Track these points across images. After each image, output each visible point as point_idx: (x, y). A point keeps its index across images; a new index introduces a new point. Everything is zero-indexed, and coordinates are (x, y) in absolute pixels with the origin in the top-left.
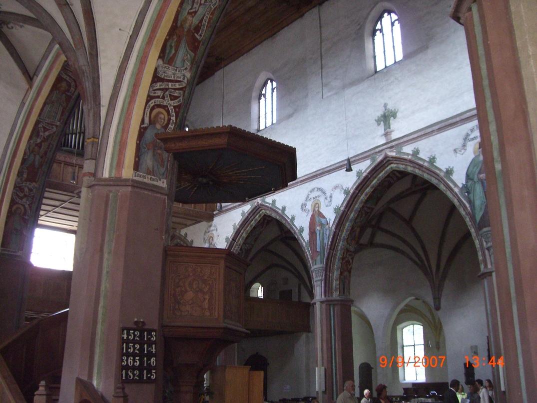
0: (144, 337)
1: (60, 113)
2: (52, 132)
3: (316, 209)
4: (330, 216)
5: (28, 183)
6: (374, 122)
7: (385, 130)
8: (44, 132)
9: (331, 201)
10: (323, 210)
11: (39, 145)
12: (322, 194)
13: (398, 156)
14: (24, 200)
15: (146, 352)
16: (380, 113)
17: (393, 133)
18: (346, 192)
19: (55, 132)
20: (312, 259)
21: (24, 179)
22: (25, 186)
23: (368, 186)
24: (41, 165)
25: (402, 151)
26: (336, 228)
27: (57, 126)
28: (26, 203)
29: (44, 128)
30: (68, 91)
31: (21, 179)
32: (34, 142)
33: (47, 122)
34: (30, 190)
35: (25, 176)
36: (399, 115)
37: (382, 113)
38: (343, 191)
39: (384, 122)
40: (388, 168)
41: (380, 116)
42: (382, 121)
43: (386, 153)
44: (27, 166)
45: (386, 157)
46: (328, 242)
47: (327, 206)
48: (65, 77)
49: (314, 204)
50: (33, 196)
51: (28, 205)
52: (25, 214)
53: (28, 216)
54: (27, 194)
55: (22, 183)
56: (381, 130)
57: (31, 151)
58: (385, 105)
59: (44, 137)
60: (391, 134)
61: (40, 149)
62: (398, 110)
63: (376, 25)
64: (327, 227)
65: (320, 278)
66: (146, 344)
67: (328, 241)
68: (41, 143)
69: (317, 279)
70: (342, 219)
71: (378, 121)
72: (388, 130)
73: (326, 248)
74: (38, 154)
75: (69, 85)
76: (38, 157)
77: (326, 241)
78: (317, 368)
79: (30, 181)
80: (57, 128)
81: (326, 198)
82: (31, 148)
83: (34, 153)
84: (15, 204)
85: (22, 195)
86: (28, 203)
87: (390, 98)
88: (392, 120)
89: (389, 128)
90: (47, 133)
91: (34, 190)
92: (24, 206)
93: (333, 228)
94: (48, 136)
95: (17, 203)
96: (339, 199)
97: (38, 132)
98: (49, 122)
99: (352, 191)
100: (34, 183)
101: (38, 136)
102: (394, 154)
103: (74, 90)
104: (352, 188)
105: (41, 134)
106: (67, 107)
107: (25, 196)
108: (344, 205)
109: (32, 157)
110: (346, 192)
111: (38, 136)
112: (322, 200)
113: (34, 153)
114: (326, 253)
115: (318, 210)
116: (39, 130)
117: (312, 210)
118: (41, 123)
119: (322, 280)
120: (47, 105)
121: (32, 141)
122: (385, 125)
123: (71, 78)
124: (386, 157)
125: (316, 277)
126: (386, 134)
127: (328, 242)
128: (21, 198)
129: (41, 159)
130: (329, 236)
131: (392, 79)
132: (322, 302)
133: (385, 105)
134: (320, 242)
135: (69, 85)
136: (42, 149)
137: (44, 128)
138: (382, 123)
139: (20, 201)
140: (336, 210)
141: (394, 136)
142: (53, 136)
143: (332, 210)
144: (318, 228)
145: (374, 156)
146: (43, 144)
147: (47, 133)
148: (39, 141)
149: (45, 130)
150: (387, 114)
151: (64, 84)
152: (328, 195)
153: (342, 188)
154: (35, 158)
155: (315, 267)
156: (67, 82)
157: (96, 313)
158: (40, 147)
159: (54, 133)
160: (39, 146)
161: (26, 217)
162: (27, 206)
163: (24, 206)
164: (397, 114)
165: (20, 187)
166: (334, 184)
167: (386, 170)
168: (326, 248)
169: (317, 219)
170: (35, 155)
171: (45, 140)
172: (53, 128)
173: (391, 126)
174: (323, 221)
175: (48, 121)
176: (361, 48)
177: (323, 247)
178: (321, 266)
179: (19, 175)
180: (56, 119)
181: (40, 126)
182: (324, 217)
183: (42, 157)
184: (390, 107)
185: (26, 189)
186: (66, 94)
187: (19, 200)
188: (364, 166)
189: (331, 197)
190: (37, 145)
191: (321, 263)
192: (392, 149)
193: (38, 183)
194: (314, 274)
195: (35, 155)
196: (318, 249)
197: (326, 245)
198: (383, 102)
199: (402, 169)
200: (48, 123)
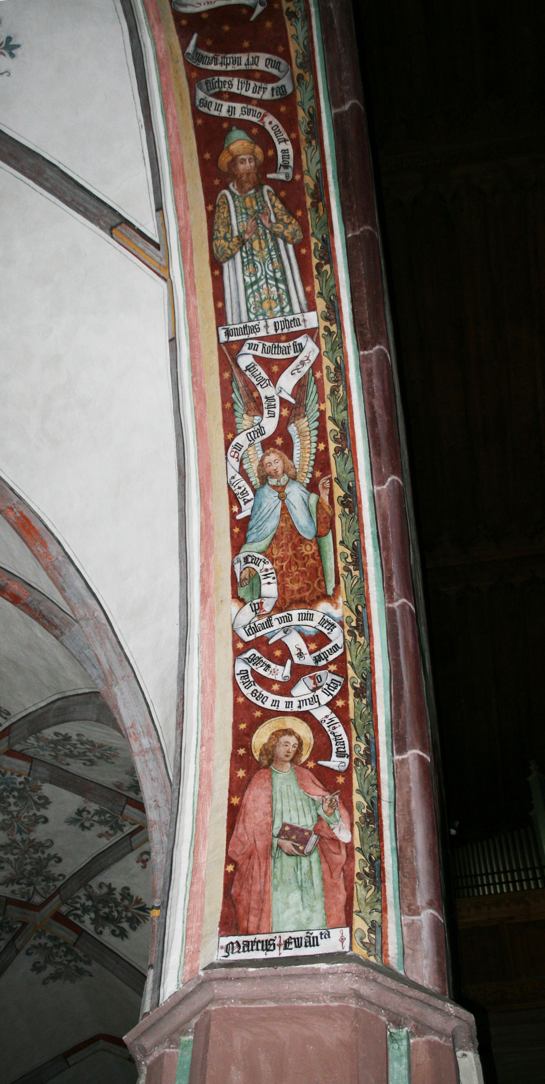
2: (305, 369)
5: (295, 613)
8: (274, 378)
11: (279, 441)
14: (302, 690)
19: (319, 357)
21: (268, 606)
22: (286, 631)
24: (325, 523)
27: (311, 333)
28: (315, 700)
29: (265, 363)
30: (270, 163)
31: (257, 609)
32: (252, 441)
33: (262, 333)
34: (320, 640)
35: (270, 590)
44: (263, 545)
48: (224, 109)
50: (341, 661)
51: (328, 704)
52: (323, 748)
53: (340, 754)
54: (308, 660)
57: (255, 480)
59: (282, 401)
61: (291, 457)
68: (282, 430)
74: (294, 478)
75: (262, 139)
76: (296, 494)
79: (299, 603)
80: (318, 343)
84: (254, 725)
85: (281, 673)
86: (325, 699)
90: (288, 381)
91: (337, 636)
92: (306, 716)
94: (301, 387)
95: (268, 715)
97: (250, 389)
98: (272, 331)
100: (324, 606)
101: (256, 406)
103: (288, 146)
105: (266, 392)
106: (305, 230)
107: (299, 672)
109: (270, 499)
111: (256, 406)
113: (273, 482)
116: (248, 383)
118: (245, 349)
120: (227, 267)
121: (241, 439)
123: (247, 100)
128: (286, 689)
129: (314, 497)
135: (262, 139)
137: (265, 363)
142: (319, 383)
146: (292, 429)
147: (288, 381)
149: (274, 370)
151: (238, 142)
154: (283, 497)
158: (288, 448)
160: (281, 442)
161: (335, 763)
162: (322, 713)
163: (306, 716)
165: (260, 643)
170: (281, 491)
171: (294, 409)
172: (301, 348)
175: (267, 328)
179: (242, 592)
180: (296, 308)
181: (244, 361)
183: (312, 487)
185: (294, 642)
186: (272, 182)
187: (272, 697)
190: (267, 444)
193: (341, 600)
195: (281, 491)
200: (275, 338)
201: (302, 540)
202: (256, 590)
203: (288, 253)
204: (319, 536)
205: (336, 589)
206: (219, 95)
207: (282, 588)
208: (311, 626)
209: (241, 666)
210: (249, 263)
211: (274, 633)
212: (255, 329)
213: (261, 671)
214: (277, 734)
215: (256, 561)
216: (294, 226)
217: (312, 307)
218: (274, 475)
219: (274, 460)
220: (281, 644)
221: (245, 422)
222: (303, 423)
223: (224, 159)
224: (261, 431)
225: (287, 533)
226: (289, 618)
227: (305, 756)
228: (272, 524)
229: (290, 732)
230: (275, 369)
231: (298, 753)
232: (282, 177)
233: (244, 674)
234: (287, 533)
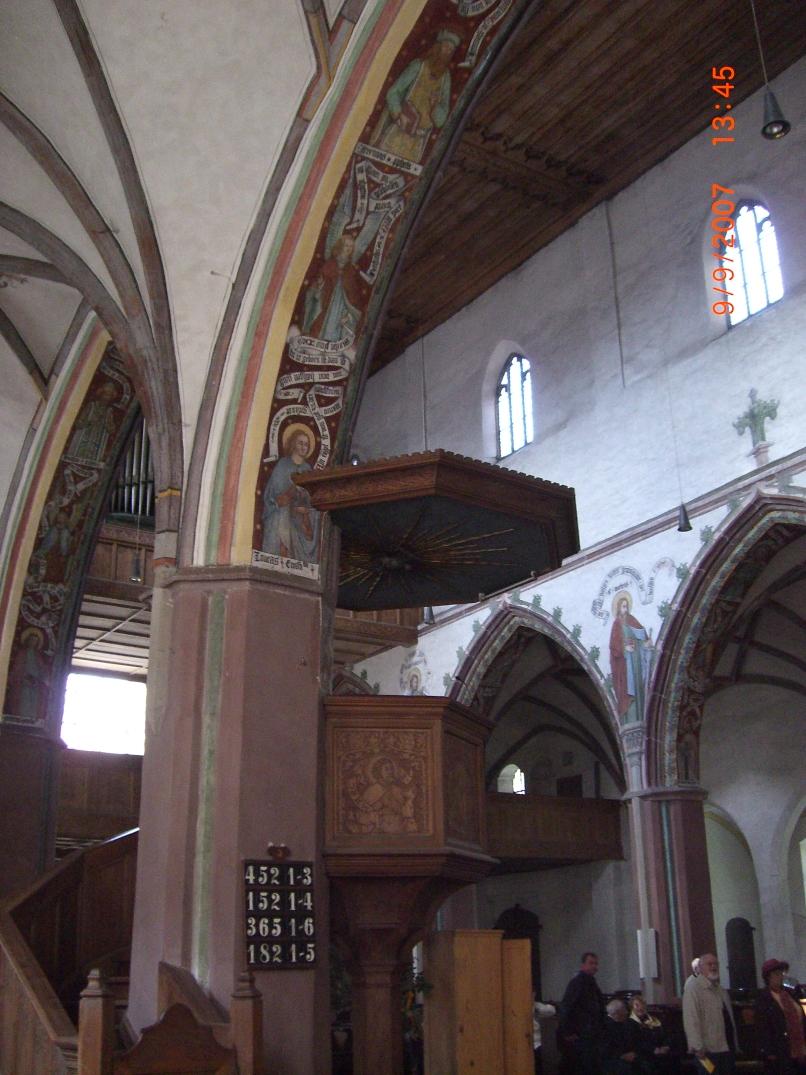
0: (291, 956)
1: (103, 446)
3: (623, 610)
4: (652, 623)
5: (49, 585)
6: (732, 428)
7: (754, 444)
8: (76, 483)
9: (651, 593)
10: (637, 612)
12: (634, 580)
13: (784, 494)
14: (43, 618)
15: (293, 934)
16: (742, 409)
17: (770, 448)
18: (682, 573)
19: (97, 483)
20: (619, 712)
22: (44, 592)
23: (725, 559)
24: (72, 551)
25: (791, 485)
26: (665, 648)
27: (99, 471)
30: (118, 400)
31: (36, 578)
34: (54, 599)
35: (43, 571)
36: (781, 411)
37: (747, 410)
38: (675, 571)
39: (750, 427)
40: (764, 521)
41: (742, 415)
42: (747, 425)
43: (758, 492)
45: (759, 498)
46: (650, 675)
47: (644, 603)
48: (109, 372)
49: (617, 600)
50: (61, 611)
52: (46, 647)
54: (49, 607)
55: (38, 587)
56: (746, 444)
57: (51, 522)
58: (753, 394)
60: (767, 452)
62: (779, 402)
63: (724, 234)
64: (646, 645)
65: (637, 749)
66: (295, 943)
67: (649, 674)
68: (70, 506)
69: (630, 751)
70: (675, 626)
71: (739, 427)
72: (761, 443)
73: (646, 686)
74: (67, 527)
75: (120, 390)
76: (66, 534)
77: (645, 674)
78: (639, 932)
81: (641, 587)
82: (52, 517)
83: (58, 525)
85: (38, 609)
86: (51, 625)
87: (761, 378)
88: (767, 423)
89: (763, 439)
90: (81, 486)
91: (62, 599)
92: (42, 630)
93: (659, 647)
94: (85, 490)
95: (30, 626)
96: (668, 588)
98: (84, 463)
99: (693, 571)
100: (61, 586)
101: (64, 492)
102: (774, 492)
103: (128, 397)
104: (693, 564)
105: (71, 487)
107: (44, 611)
108: (679, 599)
110: (682, 573)
111: (64, 492)
112: (633, 591)
114: (647, 698)
115: (627, 613)
116: (64, 481)
117: (615, 612)
119: (640, 753)
120: (78, 432)
121: (52, 503)
122: (754, 432)
123: (122, 373)
124: (759, 498)
125: (628, 748)
126: (757, 452)
127: (650, 675)
128: (38, 616)
129: (72, 538)
130: (652, 661)
131: (764, 339)
132: (643, 797)
133: (753, 394)
134: (635, 677)
135: (120, 390)
136: (72, 517)
138: (747, 429)
139: (36, 620)
140: (664, 611)
141: (774, 454)
142: (93, 492)
143: (655, 612)
144: (628, 648)
145: (734, 497)
146: (75, 507)
147: (81, 486)
148: (66, 501)
149: (77, 479)
150: (756, 411)
151: (109, 388)
152: (646, 580)
153: (673, 566)
154: (60, 533)
155: (627, 726)
156: (115, 382)
157: (189, 875)
158: (69, 514)
159: (95, 485)
160: (67, 510)
161: (49, 653)
162: (49, 631)
163: (42, 630)
164: (778, 410)
165: (33, 594)
166: (657, 558)
167: (759, 524)
168: (646, 686)
169: (625, 629)
170: (59, 529)
171: (78, 499)
172: (92, 475)
173: (767, 435)
174: (638, 634)
175: (82, 461)
176: (696, 282)
177: (640, 687)
178: (637, 724)
181: (67, 472)
182: (640, 627)
183: (73, 534)
184: (763, 396)
185: (46, 598)
187: (32, 618)
188: (716, 519)
189: (651, 584)
190: (62, 509)
191: (638, 719)
192: (770, 482)
194: (624, 741)
196: (631, 691)
197: (647, 680)
198: (746, 386)
199: (794, 522)
200: (84, 467)
201: (60, 555)
202: (37, 570)
203: (105, 436)
204: (68, 556)
205: (67, 580)
206: (112, 368)
207: (48, 572)
208: (55, 592)
209: (24, 602)
210: (88, 433)
211: (39, 591)
212: (77, 461)
213: (31, 606)
214: (32, 635)
215: (41, 558)
216: (114, 427)
217: (104, 461)
218: (59, 523)
219: (62, 516)
220: (41, 598)
221: (57, 496)
222: (80, 505)
223: (99, 391)
224: (61, 503)
225: (57, 547)
226: (46, 587)
227: (40, 647)
228: (51, 544)
229: (36, 636)
230: (78, 479)
231: (37, 645)
232: (119, 407)
233: (24, 605)
234: (57, 547)
